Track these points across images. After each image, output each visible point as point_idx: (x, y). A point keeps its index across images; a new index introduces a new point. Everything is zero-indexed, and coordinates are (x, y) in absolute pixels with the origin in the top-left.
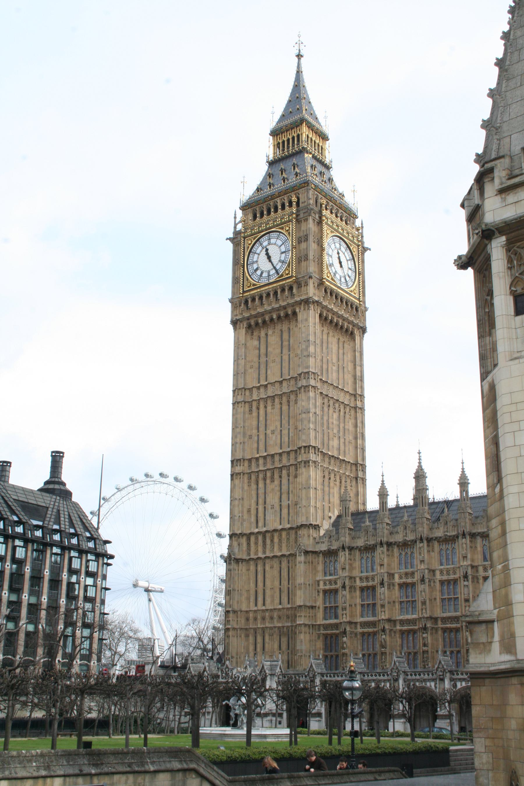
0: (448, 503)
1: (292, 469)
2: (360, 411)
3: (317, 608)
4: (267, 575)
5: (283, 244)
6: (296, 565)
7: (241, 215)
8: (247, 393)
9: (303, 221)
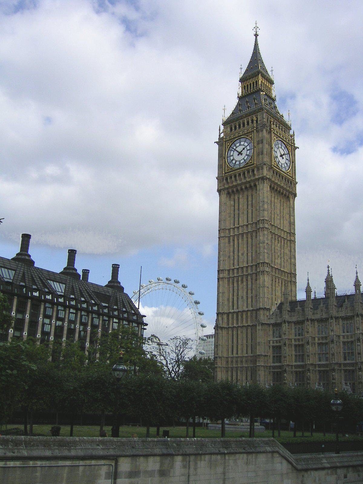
0: (348, 297)
1: (254, 276)
3: (268, 356)
4: (239, 337)
5: (248, 145)
6: (256, 331)
7: (223, 129)
8: (227, 231)
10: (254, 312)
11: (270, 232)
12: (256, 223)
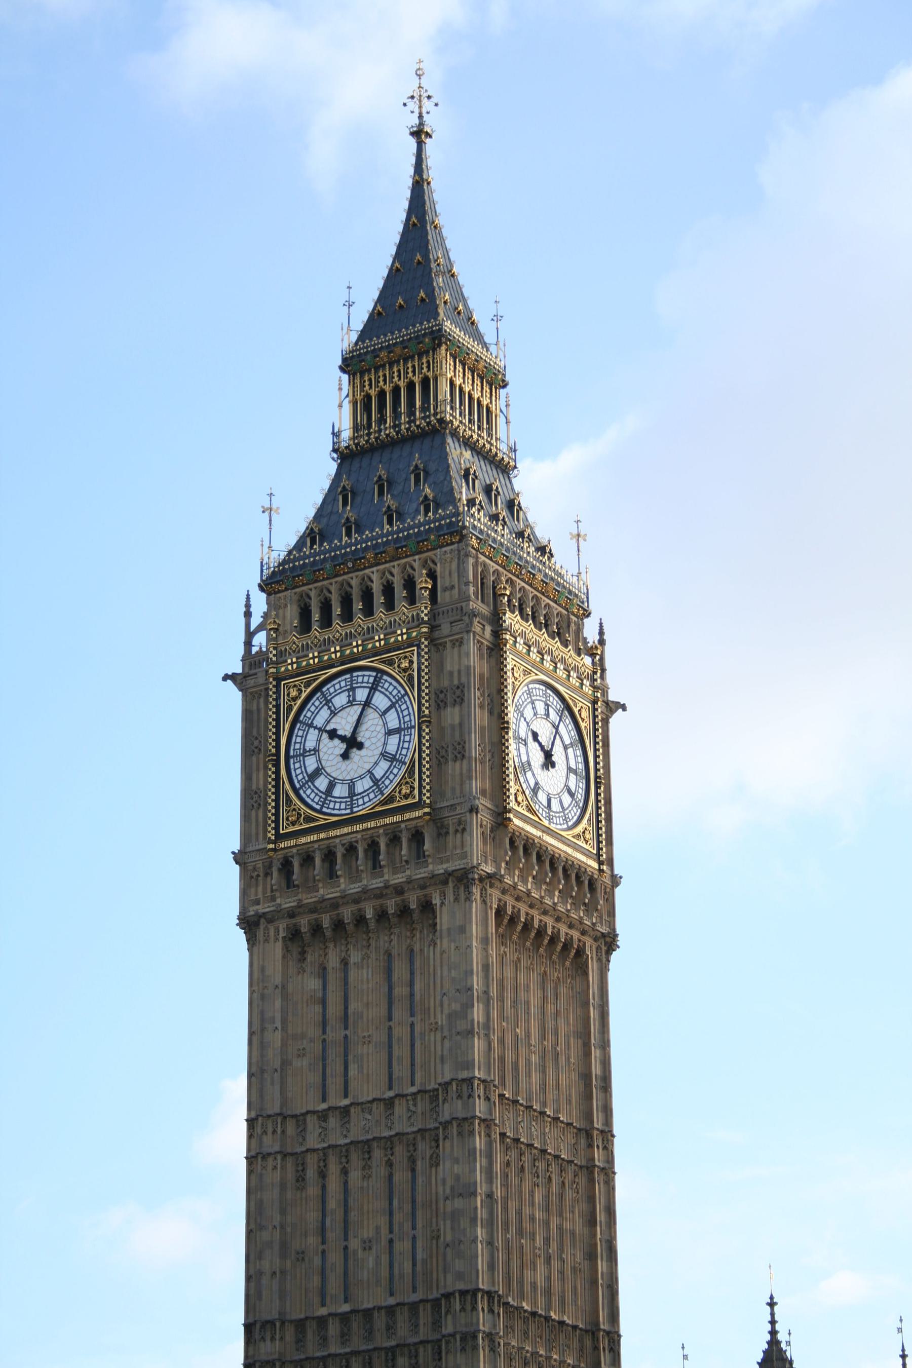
7: (265, 608)
8: (291, 1129)
9: (449, 645)
12: (433, 1096)
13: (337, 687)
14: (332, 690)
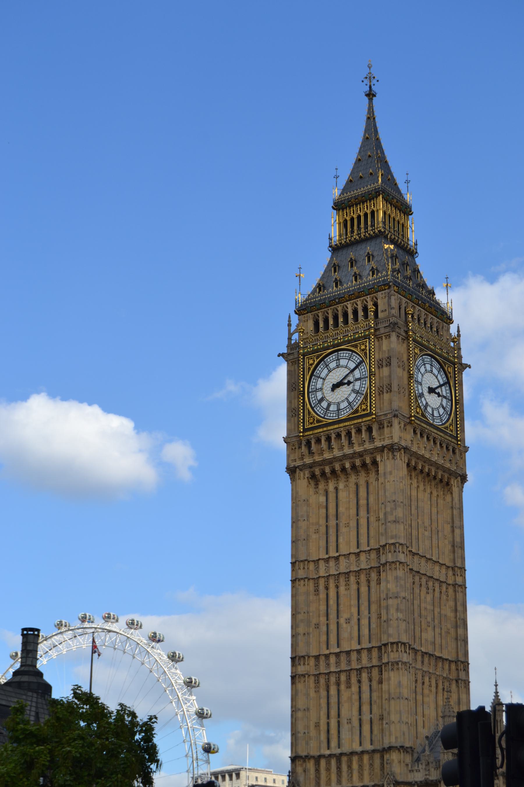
1: (375, 672)
2: (460, 589)
7: (297, 322)
8: (312, 566)
9: (384, 338)
10: (377, 756)
11: (410, 569)
12: (378, 550)
13: (331, 358)
14: (329, 360)
